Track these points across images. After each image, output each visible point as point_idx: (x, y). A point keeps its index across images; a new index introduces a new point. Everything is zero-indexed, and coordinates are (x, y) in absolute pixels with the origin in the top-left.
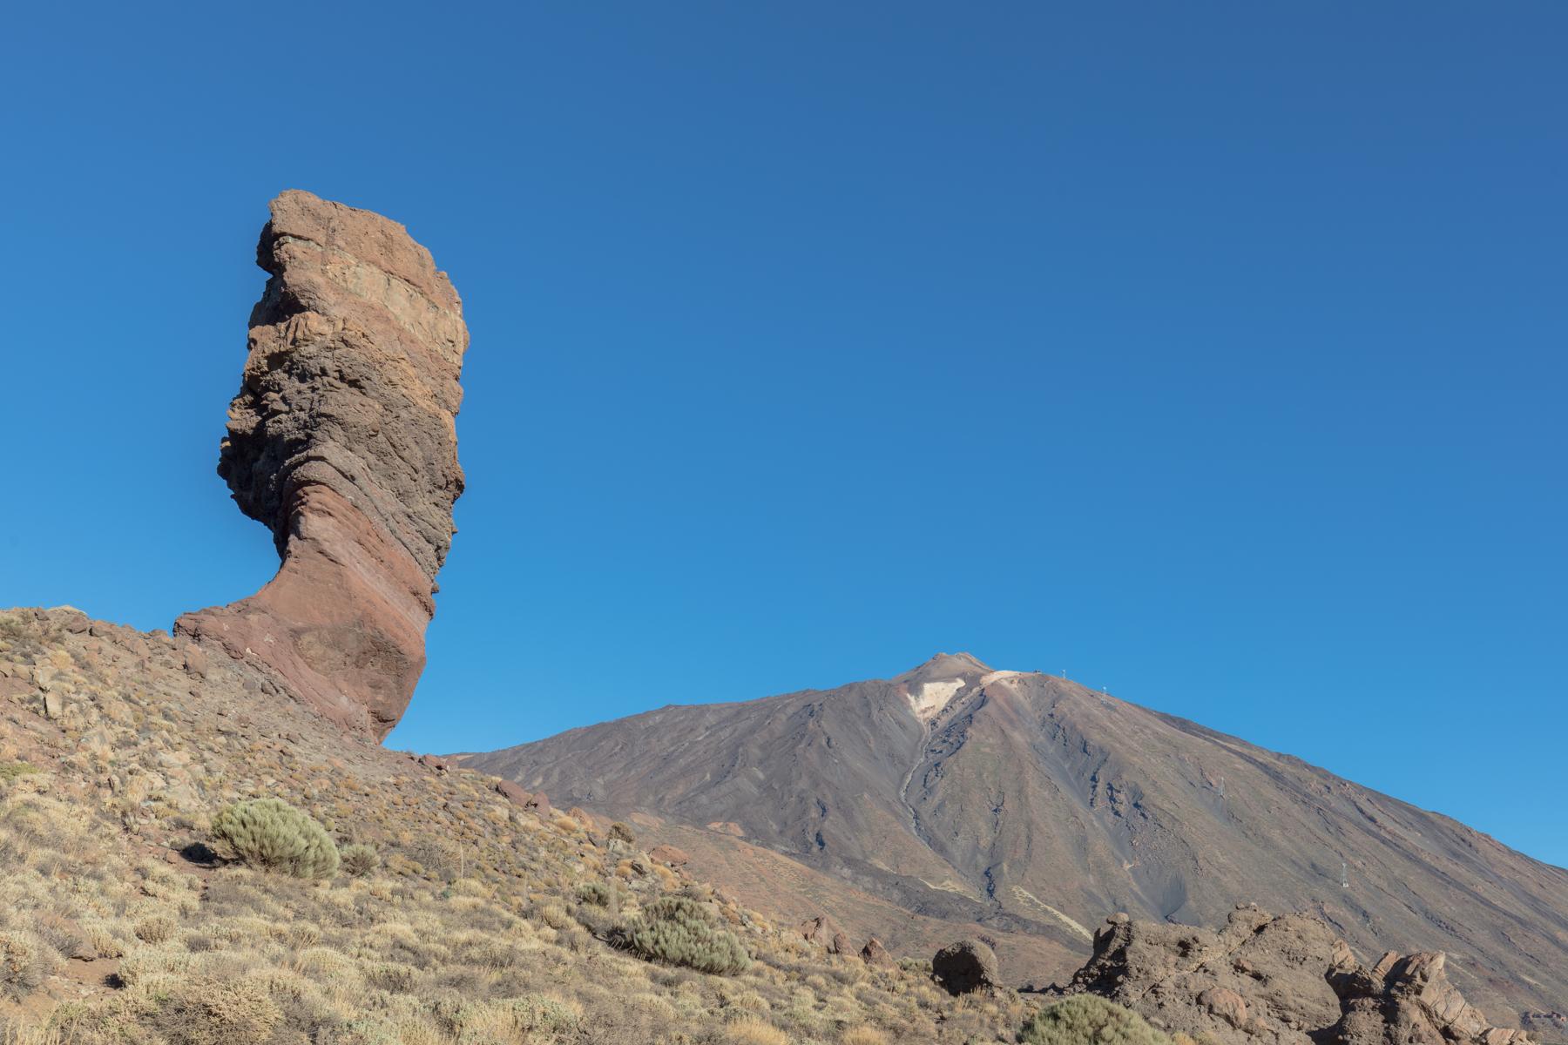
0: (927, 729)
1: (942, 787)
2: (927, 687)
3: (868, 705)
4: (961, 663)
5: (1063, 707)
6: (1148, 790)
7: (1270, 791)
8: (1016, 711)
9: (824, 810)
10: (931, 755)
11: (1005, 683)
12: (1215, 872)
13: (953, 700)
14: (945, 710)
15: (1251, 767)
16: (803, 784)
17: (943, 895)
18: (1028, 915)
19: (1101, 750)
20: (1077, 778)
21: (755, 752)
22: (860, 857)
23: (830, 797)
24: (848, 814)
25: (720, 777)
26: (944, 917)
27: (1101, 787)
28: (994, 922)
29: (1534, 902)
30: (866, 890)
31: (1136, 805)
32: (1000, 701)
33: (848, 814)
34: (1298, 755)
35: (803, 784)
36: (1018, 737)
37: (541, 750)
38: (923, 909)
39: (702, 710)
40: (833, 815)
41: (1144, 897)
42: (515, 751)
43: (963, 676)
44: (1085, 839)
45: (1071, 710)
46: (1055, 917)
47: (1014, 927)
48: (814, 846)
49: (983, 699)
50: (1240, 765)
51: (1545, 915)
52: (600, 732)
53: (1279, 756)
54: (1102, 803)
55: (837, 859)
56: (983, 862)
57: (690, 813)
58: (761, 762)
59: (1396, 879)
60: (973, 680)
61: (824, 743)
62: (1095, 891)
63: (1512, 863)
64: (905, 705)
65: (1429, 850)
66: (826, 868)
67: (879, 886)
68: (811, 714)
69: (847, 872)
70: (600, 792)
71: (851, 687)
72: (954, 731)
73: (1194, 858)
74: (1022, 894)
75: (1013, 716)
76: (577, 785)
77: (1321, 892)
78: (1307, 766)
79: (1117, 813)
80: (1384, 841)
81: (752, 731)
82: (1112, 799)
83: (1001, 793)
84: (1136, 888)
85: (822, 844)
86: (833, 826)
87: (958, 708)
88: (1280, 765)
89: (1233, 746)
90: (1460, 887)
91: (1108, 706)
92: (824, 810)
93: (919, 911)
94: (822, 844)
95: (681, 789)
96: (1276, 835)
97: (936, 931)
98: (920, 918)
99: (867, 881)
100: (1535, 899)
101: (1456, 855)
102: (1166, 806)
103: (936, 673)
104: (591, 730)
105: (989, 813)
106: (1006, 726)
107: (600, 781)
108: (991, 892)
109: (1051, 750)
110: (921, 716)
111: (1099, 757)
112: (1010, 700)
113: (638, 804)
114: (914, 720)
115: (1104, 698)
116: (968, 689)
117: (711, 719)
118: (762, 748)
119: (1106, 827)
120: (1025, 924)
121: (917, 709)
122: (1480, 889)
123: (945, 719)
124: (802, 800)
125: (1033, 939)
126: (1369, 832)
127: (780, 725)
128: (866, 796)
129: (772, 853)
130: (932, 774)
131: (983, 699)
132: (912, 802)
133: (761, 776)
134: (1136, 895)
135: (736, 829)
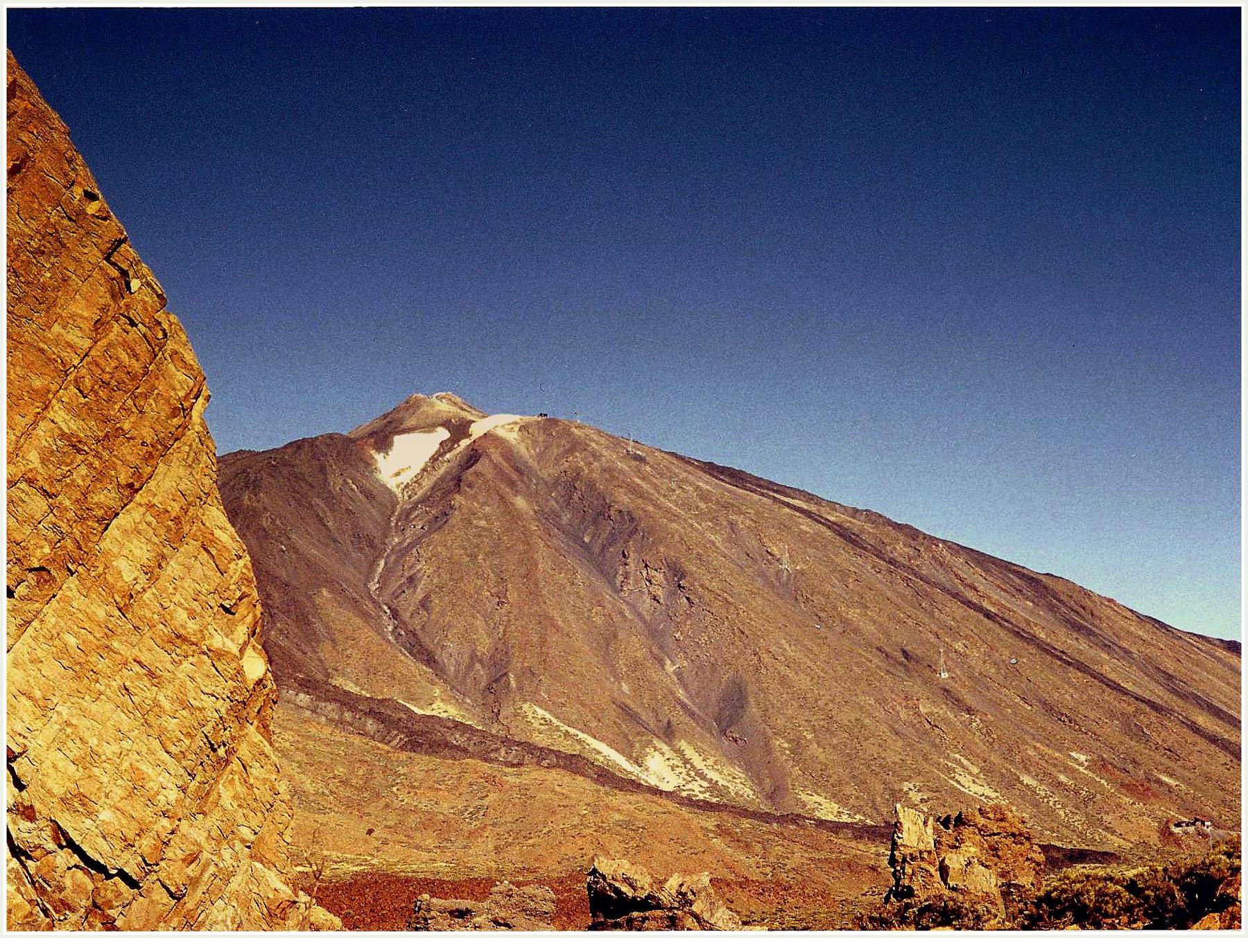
3: (322, 469)
7: (845, 557)
8: (517, 470)
11: (501, 433)
13: (434, 459)
14: (424, 470)
22: (320, 677)
31: (679, 586)
33: (303, 620)
36: (520, 502)
43: (446, 424)
46: (579, 741)
50: (806, 526)
51: (1184, 696)
60: (459, 429)
62: (628, 702)
64: (369, 464)
65: (1045, 628)
67: (348, 716)
69: (303, 699)
71: (297, 446)
75: (514, 476)
77: (914, 687)
78: (889, 523)
80: (988, 615)
84: (681, 693)
88: (857, 524)
90: (1081, 667)
91: (637, 458)
96: (853, 614)
100: (1170, 677)
101: (1077, 628)
102: (715, 585)
110: (392, 483)
112: (509, 454)
120: (540, 755)
122: (1106, 670)
123: (427, 483)
126: (969, 604)
131: (473, 456)
132: (386, 596)
134: (684, 706)
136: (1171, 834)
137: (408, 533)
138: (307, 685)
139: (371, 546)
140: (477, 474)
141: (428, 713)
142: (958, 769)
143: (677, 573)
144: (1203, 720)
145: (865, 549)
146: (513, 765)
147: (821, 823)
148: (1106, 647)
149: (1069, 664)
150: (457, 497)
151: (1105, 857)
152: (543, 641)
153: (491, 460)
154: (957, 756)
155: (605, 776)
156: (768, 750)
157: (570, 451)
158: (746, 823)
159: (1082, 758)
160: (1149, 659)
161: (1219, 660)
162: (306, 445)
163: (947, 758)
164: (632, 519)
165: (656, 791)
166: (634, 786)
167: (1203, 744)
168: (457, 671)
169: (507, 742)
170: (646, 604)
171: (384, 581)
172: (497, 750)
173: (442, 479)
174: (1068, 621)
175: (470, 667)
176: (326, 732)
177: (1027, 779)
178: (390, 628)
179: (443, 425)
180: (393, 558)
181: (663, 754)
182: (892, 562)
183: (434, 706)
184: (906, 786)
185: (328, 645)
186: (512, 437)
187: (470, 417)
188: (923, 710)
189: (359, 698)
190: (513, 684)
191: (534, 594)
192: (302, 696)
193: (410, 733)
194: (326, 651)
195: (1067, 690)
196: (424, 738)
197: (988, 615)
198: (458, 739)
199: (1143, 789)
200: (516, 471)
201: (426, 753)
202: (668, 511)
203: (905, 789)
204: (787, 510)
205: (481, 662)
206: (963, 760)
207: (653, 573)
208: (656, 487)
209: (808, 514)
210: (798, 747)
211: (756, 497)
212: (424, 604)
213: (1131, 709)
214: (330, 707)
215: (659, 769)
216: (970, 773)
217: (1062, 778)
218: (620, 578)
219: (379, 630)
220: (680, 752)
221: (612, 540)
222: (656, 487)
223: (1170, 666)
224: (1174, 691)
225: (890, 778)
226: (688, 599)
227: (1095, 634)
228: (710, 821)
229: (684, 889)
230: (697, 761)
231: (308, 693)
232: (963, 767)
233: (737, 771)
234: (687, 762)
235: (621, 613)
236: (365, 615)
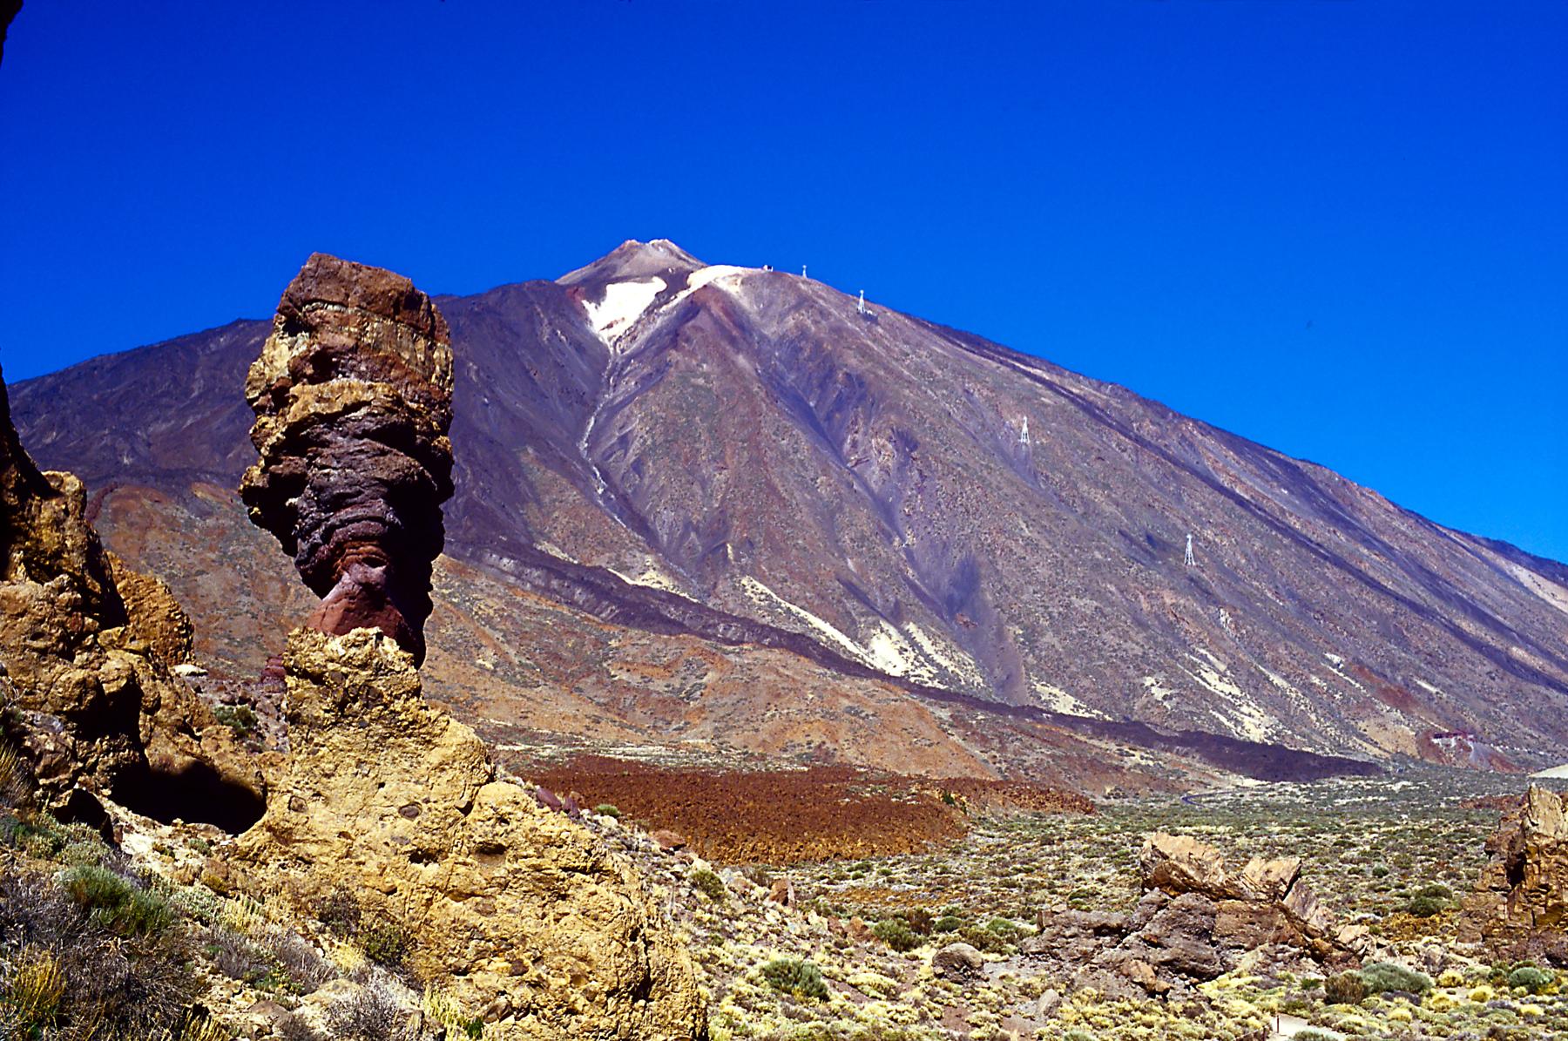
3: (531, 318)
4: (659, 252)
7: (1087, 434)
12: (1021, 552)
13: (650, 311)
14: (638, 322)
15: (1064, 401)
20: (829, 418)
22: (523, 540)
29: (1432, 581)
30: (535, 587)
32: (716, 310)
36: (741, 360)
37: (55, 389)
43: (662, 274)
44: (840, 508)
45: (816, 322)
46: (802, 621)
50: (1048, 398)
51: (1448, 598)
52: (141, 356)
59: (1256, 554)
60: (676, 281)
62: (854, 580)
63: (1403, 528)
67: (555, 583)
69: (507, 563)
71: (504, 290)
89: (1038, 372)
90: (1339, 562)
91: (867, 317)
96: (1098, 496)
100: (1433, 576)
106: (724, 344)
110: (604, 336)
112: (730, 308)
114: (595, 339)
123: (642, 338)
131: (693, 308)
134: (913, 587)
136: (1431, 745)
137: (621, 389)
139: (585, 404)
140: (697, 329)
141: (640, 583)
142: (1205, 666)
143: (906, 442)
144: (1468, 626)
145: (1110, 425)
146: (732, 643)
147: (1060, 718)
148: (1369, 540)
149: (1326, 558)
150: (673, 352)
151: (1365, 769)
153: (711, 315)
154: (1203, 651)
156: (1000, 635)
157: (797, 308)
159: (1336, 659)
160: (1412, 558)
161: (1485, 560)
162: (513, 293)
163: (1192, 652)
164: (861, 384)
165: (881, 675)
166: (858, 669)
167: (1466, 651)
168: (670, 542)
169: (723, 616)
171: (594, 441)
172: (715, 626)
173: (658, 333)
174: (1325, 512)
175: (684, 536)
176: (530, 601)
177: (1277, 680)
178: (600, 491)
179: (658, 275)
180: (601, 420)
181: (890, 637)
182: (1138, 440)
183: (646, 576)
184: (1149, 681)
185: (533, 506)
186: (734, 290)
187: (688, 267)
188: (1168, 601)
189: (568, 565)
190: (731, 556)
191: (757, 461)
192: (505, 560)
193: (621, 603)
194: (531, 512)
195: (1325, 585)
196: (641, 610)
197: (1241, 502)
198: (672, 612)
199: (1403, 698)
200: (736, 326)
201: (639, 626)
202: (900, 376)
203: (1147, 684)
204: (1027, 380)
205: (696, 530)
206: (1211, 657)
207: (882, 441)
208: (887, 349)
209: (1050, 385)
210: (1032, 634)
211: (995, 365)
212: (637, 467)
213: (1391, 610)
214: (536, 574)
215: (885, 651)
216: (1218, 672)
217: (1315, 680)
218: (847, 446)
219: (587, 492)
220: (907, 635)
221: (840, 404)
222: (887, 349)
223: (1434, 567)
224: (1438, 593)
226: (920, 472)
227: (1355, 528)
228: (945, 714)
229: (1272, 878)
230: (928, 647)
231: (512, 558)
232: (1209, 663)
233: (967, 658)
234: (914, 644)
236: (574, 479)
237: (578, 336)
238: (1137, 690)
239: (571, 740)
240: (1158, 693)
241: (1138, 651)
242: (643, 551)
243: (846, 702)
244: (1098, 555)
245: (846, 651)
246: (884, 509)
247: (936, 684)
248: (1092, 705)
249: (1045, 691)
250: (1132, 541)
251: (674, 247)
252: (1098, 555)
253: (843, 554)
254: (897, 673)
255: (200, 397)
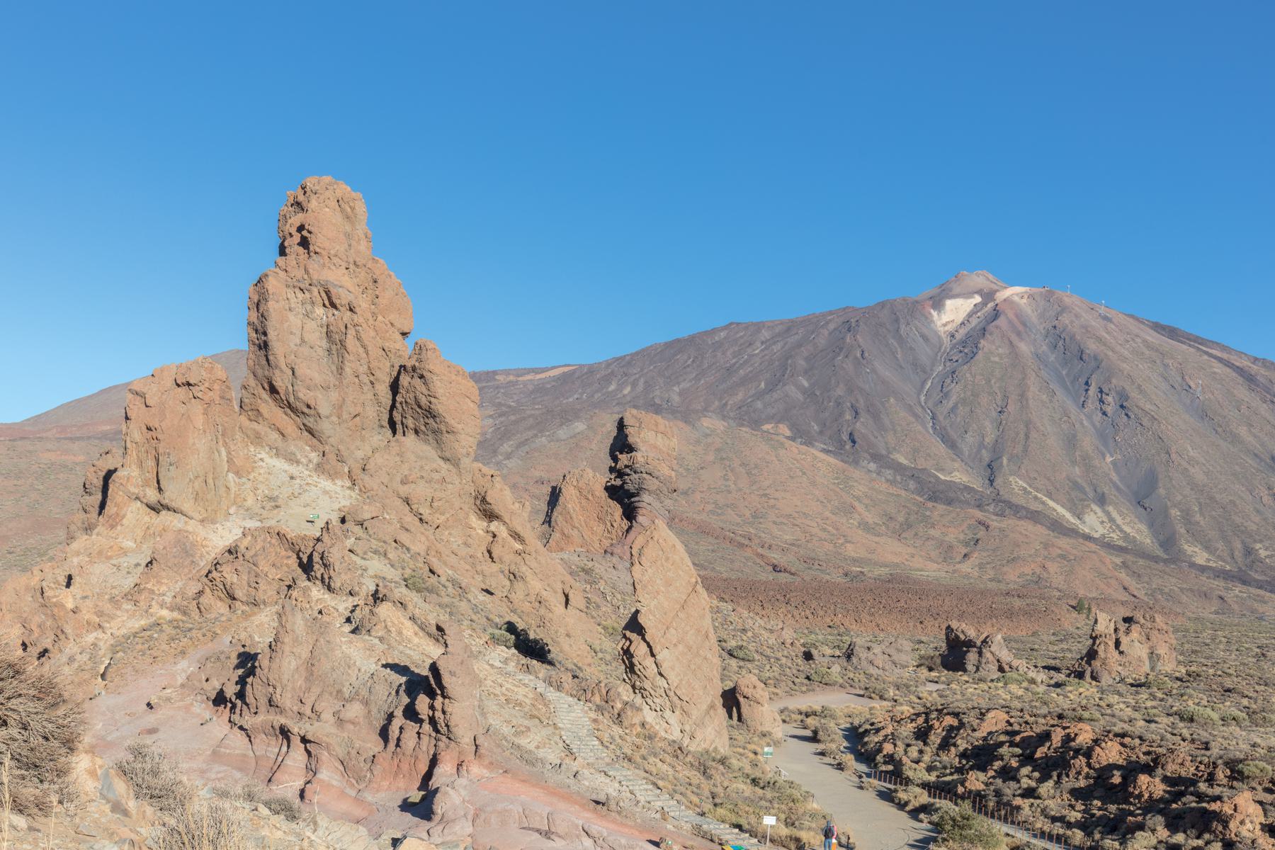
0: (947, 341)
1: (956, 391)
2: (949, 303)
3: (897, 320)
4: (980, 279)
5: (1065, 319)
6: (1134, 394)
7: (1242, 392)
8: (1024, 325)
9: (857, 413)
10: (948, 364)
11: (1016, 299)
12: (1185, 464)
13: (970, 315)
14: (963, 323)
15: (1228, 370)
16: (840, 391)
17: (951, 485)
18: (1022, 502)
19: (1096, 358)
20: (1072, 382)
21: (802, 363)
22: (884, 452)
23: (861, 401)
24: (876, 417)
25: (772, 386)
26: (949, 504)
27: (1093, 390)
28: (991, 508)
30: (887, 480)
31: (1122, 406)
32: (1011, 315)
33: (876, 417)
34: (1268, 358)
35: (840, 391)
36: (1024, 347)
37: (629, 363)
38: (934, 498)
39: (759, 327)
40: (864, 417)
41: (1121, 486)
42: (608, 364)
43: (980, 292)
44: (1074, 436)
45: (1072, 322)
46: (1043, 503)
47: (1008, 511)
48: (848, 445)
49: (996, 314)
50: (1219, 368)
52: (676, 346)
53: (1256, 360)
54: (1092, 404)
55: (866, 455)
56: (986, 456)
57: (749, 417)
58: (806, 372)
60: (988, 296)
61: (859, 355)
62: (1079, 480)
64: (928, 319)
66: (856, 463)
67: (898, 478)
68: (849, 330)
69: (873, 466)
70: (676, 399)
71: (882, 305)
72: (969, 342)
73: (1167, 453)
74: (1017, 483)
75: (1021, 328)
76: (657, 393)
79: (1104, 413)
81: (799, 345)
82: (1101, 401)
83: (1006, 397)
84: (1115, 478)
85: (854, 442)
86: (863, 426)
87: (974, 322)
88: (1255, 368)
91: (1106, 318)
92: (857, 413)
93: (930, 499)
94: (854, 442)
95: (740, 396)
96: (1243, 431)
97: (942, 516)
98: (930, 504)
99: (888, 473)
102: (1148, 407)
103: (957, 290)
104: (669, 345)
105: (994, 414)
106: (1014, 338)
107: (676, 389)
108: (991, 482)
109: (1052, 358)
110: (942, 329)
111: (1093, 364)
113: (705, 409)
114: (936, 333)
115: (1102, 310)
116: (984, 304)
117: (765, 334)
118: (807, 359)
119: (1094, 425)
120: (1016, 510)
121: (939, 323)
123: (963, 331)
124: (838, 404)
125: (1022, 522)
127: (822, 341)
128: (892, 400)
129: (813, 450)
130: (948, 381)
131: (996, 314)
132: (930, 404)
133: (806, 384)
135: (785, 430)
138: (876, 457)
140: (997, 327)
152: (1027, 436)
155: (1058, 527)
158: (1141, 562)
165: (1088, 538)
166: (1072, 532)
170: (1098, 417)
175: (979, 451)
176: (885, 485)
184: (1258, 546)
187: (995, 287)
204: (1206, 357)
205: (985, 448)
211: (1185, 347)
212: (953, 409)
215: (1093, 522)
220: (1108, 514)
225: (1248, 540)
230: (1119, 520)
233: (1143, 527)
234: (1112, 520)
235: (1082, 423)
236: (916, 416)
237: (925, 331)
238: (1249, 552)
239: (897, 565)
240: (1263, 553)
241: (1254, 527)
242: (953, 460)
243: (1060, 552)
244: (1237, 468)
245: (1068, 521)
246: (1102, 436)
247: (1121, 543)
248: (1220, 558)
249: (1189, 549)
250: (1262, 460)
251: (991, 277)
252: (1237, 468)
253: (1074, 463)
254: (1096, 535)
255: (710, 367)
